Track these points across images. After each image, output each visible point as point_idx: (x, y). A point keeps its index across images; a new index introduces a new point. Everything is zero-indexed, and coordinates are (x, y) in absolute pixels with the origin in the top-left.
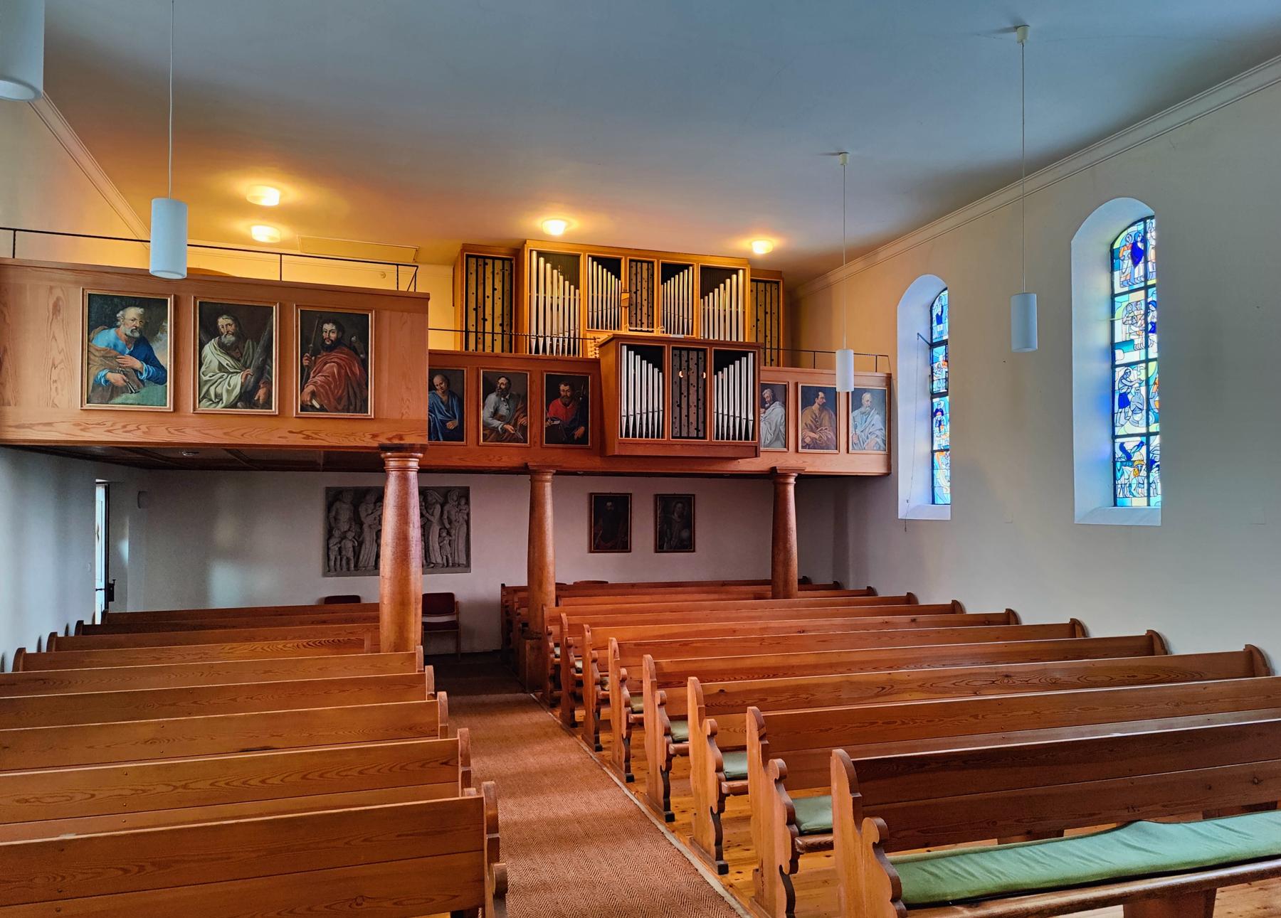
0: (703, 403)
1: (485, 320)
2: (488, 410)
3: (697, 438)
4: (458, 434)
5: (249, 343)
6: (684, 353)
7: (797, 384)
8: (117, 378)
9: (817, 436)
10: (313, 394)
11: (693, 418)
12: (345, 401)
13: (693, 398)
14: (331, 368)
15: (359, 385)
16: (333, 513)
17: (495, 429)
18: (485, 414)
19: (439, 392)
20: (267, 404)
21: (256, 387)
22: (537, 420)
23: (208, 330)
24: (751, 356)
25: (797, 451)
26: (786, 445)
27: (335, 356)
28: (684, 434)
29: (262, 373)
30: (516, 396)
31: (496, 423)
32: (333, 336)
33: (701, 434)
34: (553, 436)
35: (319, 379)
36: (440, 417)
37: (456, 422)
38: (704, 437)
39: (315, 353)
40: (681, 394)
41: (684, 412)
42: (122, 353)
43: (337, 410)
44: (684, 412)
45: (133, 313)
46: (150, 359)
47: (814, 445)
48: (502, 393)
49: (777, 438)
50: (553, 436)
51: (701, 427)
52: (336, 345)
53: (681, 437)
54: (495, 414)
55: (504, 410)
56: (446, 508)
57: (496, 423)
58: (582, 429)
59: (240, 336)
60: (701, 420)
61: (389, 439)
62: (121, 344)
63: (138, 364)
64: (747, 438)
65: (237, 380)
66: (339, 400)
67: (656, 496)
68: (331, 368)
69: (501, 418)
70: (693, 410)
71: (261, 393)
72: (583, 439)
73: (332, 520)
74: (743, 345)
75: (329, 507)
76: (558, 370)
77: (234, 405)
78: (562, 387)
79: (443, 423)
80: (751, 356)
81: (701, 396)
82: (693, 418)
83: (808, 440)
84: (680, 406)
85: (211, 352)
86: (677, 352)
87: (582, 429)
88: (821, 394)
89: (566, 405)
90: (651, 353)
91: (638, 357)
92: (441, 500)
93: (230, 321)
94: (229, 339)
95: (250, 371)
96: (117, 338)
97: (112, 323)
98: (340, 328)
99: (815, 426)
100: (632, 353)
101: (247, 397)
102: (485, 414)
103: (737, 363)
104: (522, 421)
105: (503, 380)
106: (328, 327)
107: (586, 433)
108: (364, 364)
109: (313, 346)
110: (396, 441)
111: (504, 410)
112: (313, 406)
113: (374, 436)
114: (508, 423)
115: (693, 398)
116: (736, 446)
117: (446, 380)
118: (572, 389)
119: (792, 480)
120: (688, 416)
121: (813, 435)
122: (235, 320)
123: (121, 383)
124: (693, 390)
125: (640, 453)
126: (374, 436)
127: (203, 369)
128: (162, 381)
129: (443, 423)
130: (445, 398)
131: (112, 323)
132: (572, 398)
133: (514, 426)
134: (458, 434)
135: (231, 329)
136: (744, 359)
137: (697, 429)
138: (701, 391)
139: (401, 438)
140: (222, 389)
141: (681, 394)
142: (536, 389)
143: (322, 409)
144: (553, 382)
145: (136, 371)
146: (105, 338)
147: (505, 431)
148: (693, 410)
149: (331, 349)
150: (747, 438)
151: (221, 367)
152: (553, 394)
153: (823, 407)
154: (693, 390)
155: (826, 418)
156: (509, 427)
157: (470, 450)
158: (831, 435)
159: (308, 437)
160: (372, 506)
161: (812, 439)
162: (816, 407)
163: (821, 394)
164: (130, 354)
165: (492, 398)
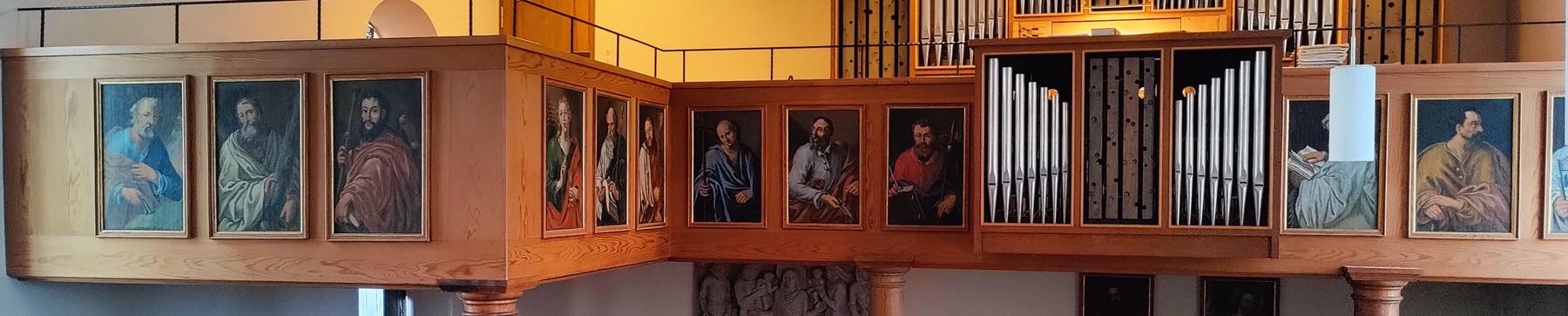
0: (1152, 153)
1: (868, 12)
2: (795, 172)
3: (1140, 220)
4: (751, 211)
5: (272, 136)
6: (1113, 64)
7: (1407, 100)
8: (131, 194)
9: (1457, 204)
10: (351, 206)
11: (1130, 184)
12: (390, 217)
13: (1131, 146)
14: (373, 166)
15: (409, 188)
16: (703, 293)
17: (807, 203)
18: (793, 179)
19: (725, 147)
20: (294, 224)
21: (281, 202)
22: (878, 180)
23: (225, 121)
24: (1260, 57)
25: (1405, 234)
26: (1378, 223)
27: (380, 147)
28: (1112, 212)
29: (288, 175)
30: (842, 146)
31: (810, 192)
32: (375, 116)
33: (1147, 214)
34: (904, 210)
35: (358, 183)
36: (726, 184)
37: (750, 193)
38: (1154, 221)
39: (353, 145)
40: (1106, 139)
41: (1112, 173)
42: (136, 160)
43: (381, 230)
44: (1112, 173)
45: (146, 105)
46: (164, 166)
47: (1451, 222)
48: (820, 145)
49: (1357, 209)
50: (904, 210)
51: (1147, 200)
52: (380, 128)
53: (1104, 220)
54: (808, 178)
55: (821, 171)
56: (853, 290)
57: (810, 192)
58: (952, 198)
59: (263, 127)
60: (1147, 186)
61: (451, 273)
62: (135, 147)
63: (151, 174)
64: (1250, 219)
65: (259, 190)
66: (383, 214)
67: (1202, 278)
68: (373, 166)
69: (818, 184)
70: (1130, 169)
71: (288, 206)
72: (953, 217)
73: (703, 302)
74: (1246, 37)
75: (698, 286)
76: (910, 100)
77: (257, 227)
78: (918, 129)
79: (732, 193)
80: (1260, 57)
81: (1148, 143)
82: (1130, 184)
83: (1434, 212)
84: (1103, 162)
85: (231, 154)
86: (1099, 62)
87: (952, 198)
88: (1471, 116)
89: (922, 158)
90: (1045, 66)
91: (1020, 78)
92: (847, 277)
93: (250, 106)
94: (250, 131)
95: (273, 176)
96: (132, 142)
97: (125, 120)
98: (384, 105)
99: (1455, 180)
100: (1008, 72)
101: (271, 217)
102: (793, 179)
103: (1229, 74)
104: (851, 188)
105: (821, 123)
106: (369, 103)
107: (958, 204)
108: (415, 155)
109: (349, 134)
110: (461, 277)
111: (821, 171)
112: (350, 225)
113: (432, 268)
114: (830, 192)
115: (1131, 146)
116: (1221, 236)
117: (735, 127)
118: (935, 131)
119: (1394, 295)
120: (1120, 180)
121: (1447, 201)
122: (257, 104)
123: (136, 201)
124: (1130, 133)
125: (1022, 250)
126: (432, 268)
127: (222, 176)
128: (178, 198)
129: (732, 193)
130: (733, 156)
131: (125, 120)
132: (934, 146)
133: (839, 196)
134: (751, 211)
135: (251, 117)
136: (1245, 66)
137: (1140, 206)
138: (1148, 132)
139: (468, 272)
140: (243, 204)
141: (1106, 139)
142: (875, 135)
143: (362, 229)
144: (902, 121)
145: (151, 183)
146: (120, 142)
147: (824, 204)
148: (1130, 169)
149: (372, 136)
150: (1250, 219)
151: (242, 174)
152: (901, 140)
153: (1475, 142)
154: (1130, 133)
155: (1484, 165)
156: (830, 199)
157: (773, 236)
158: (1496, 201)
159: (345, 270)
160: (751, 283)
161: (1446, 210)
162: (1456, 144)
163: (1471, 116)
164: (145, 162)
165: (804, 152)
